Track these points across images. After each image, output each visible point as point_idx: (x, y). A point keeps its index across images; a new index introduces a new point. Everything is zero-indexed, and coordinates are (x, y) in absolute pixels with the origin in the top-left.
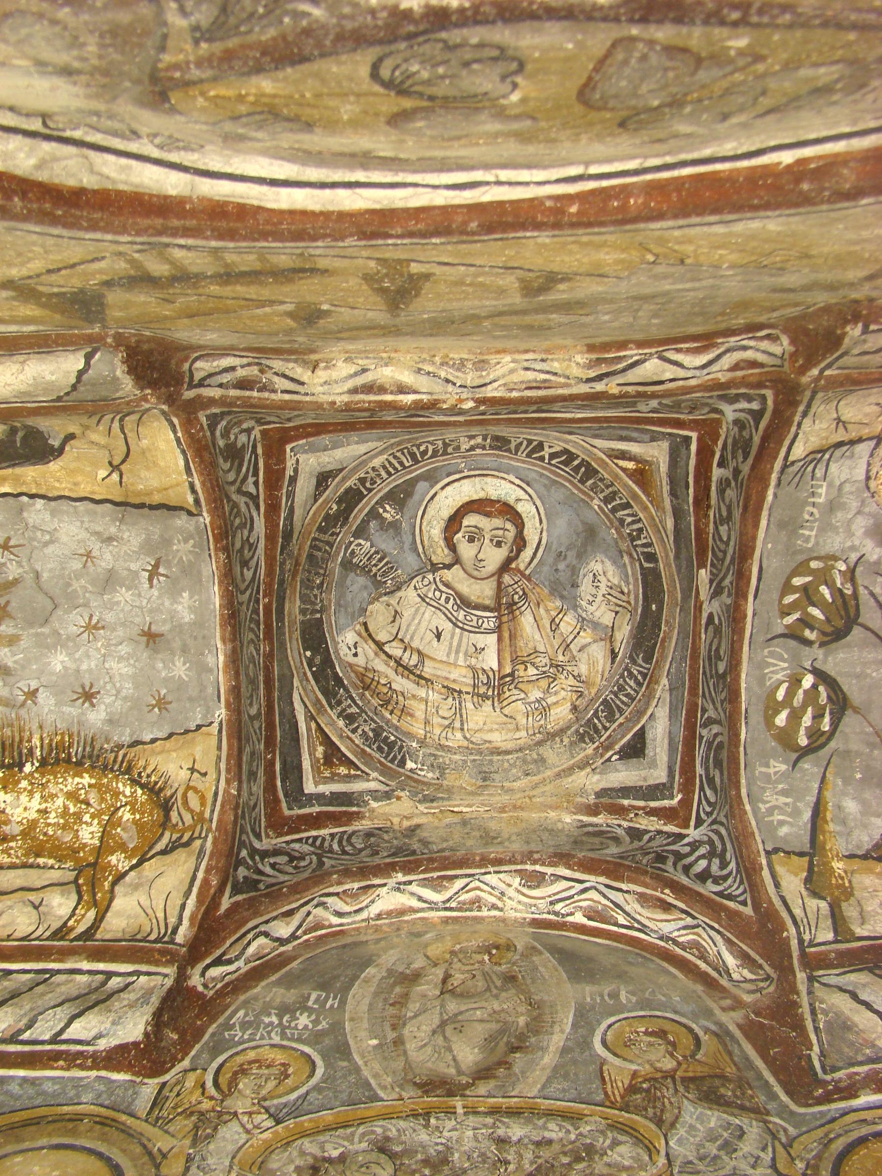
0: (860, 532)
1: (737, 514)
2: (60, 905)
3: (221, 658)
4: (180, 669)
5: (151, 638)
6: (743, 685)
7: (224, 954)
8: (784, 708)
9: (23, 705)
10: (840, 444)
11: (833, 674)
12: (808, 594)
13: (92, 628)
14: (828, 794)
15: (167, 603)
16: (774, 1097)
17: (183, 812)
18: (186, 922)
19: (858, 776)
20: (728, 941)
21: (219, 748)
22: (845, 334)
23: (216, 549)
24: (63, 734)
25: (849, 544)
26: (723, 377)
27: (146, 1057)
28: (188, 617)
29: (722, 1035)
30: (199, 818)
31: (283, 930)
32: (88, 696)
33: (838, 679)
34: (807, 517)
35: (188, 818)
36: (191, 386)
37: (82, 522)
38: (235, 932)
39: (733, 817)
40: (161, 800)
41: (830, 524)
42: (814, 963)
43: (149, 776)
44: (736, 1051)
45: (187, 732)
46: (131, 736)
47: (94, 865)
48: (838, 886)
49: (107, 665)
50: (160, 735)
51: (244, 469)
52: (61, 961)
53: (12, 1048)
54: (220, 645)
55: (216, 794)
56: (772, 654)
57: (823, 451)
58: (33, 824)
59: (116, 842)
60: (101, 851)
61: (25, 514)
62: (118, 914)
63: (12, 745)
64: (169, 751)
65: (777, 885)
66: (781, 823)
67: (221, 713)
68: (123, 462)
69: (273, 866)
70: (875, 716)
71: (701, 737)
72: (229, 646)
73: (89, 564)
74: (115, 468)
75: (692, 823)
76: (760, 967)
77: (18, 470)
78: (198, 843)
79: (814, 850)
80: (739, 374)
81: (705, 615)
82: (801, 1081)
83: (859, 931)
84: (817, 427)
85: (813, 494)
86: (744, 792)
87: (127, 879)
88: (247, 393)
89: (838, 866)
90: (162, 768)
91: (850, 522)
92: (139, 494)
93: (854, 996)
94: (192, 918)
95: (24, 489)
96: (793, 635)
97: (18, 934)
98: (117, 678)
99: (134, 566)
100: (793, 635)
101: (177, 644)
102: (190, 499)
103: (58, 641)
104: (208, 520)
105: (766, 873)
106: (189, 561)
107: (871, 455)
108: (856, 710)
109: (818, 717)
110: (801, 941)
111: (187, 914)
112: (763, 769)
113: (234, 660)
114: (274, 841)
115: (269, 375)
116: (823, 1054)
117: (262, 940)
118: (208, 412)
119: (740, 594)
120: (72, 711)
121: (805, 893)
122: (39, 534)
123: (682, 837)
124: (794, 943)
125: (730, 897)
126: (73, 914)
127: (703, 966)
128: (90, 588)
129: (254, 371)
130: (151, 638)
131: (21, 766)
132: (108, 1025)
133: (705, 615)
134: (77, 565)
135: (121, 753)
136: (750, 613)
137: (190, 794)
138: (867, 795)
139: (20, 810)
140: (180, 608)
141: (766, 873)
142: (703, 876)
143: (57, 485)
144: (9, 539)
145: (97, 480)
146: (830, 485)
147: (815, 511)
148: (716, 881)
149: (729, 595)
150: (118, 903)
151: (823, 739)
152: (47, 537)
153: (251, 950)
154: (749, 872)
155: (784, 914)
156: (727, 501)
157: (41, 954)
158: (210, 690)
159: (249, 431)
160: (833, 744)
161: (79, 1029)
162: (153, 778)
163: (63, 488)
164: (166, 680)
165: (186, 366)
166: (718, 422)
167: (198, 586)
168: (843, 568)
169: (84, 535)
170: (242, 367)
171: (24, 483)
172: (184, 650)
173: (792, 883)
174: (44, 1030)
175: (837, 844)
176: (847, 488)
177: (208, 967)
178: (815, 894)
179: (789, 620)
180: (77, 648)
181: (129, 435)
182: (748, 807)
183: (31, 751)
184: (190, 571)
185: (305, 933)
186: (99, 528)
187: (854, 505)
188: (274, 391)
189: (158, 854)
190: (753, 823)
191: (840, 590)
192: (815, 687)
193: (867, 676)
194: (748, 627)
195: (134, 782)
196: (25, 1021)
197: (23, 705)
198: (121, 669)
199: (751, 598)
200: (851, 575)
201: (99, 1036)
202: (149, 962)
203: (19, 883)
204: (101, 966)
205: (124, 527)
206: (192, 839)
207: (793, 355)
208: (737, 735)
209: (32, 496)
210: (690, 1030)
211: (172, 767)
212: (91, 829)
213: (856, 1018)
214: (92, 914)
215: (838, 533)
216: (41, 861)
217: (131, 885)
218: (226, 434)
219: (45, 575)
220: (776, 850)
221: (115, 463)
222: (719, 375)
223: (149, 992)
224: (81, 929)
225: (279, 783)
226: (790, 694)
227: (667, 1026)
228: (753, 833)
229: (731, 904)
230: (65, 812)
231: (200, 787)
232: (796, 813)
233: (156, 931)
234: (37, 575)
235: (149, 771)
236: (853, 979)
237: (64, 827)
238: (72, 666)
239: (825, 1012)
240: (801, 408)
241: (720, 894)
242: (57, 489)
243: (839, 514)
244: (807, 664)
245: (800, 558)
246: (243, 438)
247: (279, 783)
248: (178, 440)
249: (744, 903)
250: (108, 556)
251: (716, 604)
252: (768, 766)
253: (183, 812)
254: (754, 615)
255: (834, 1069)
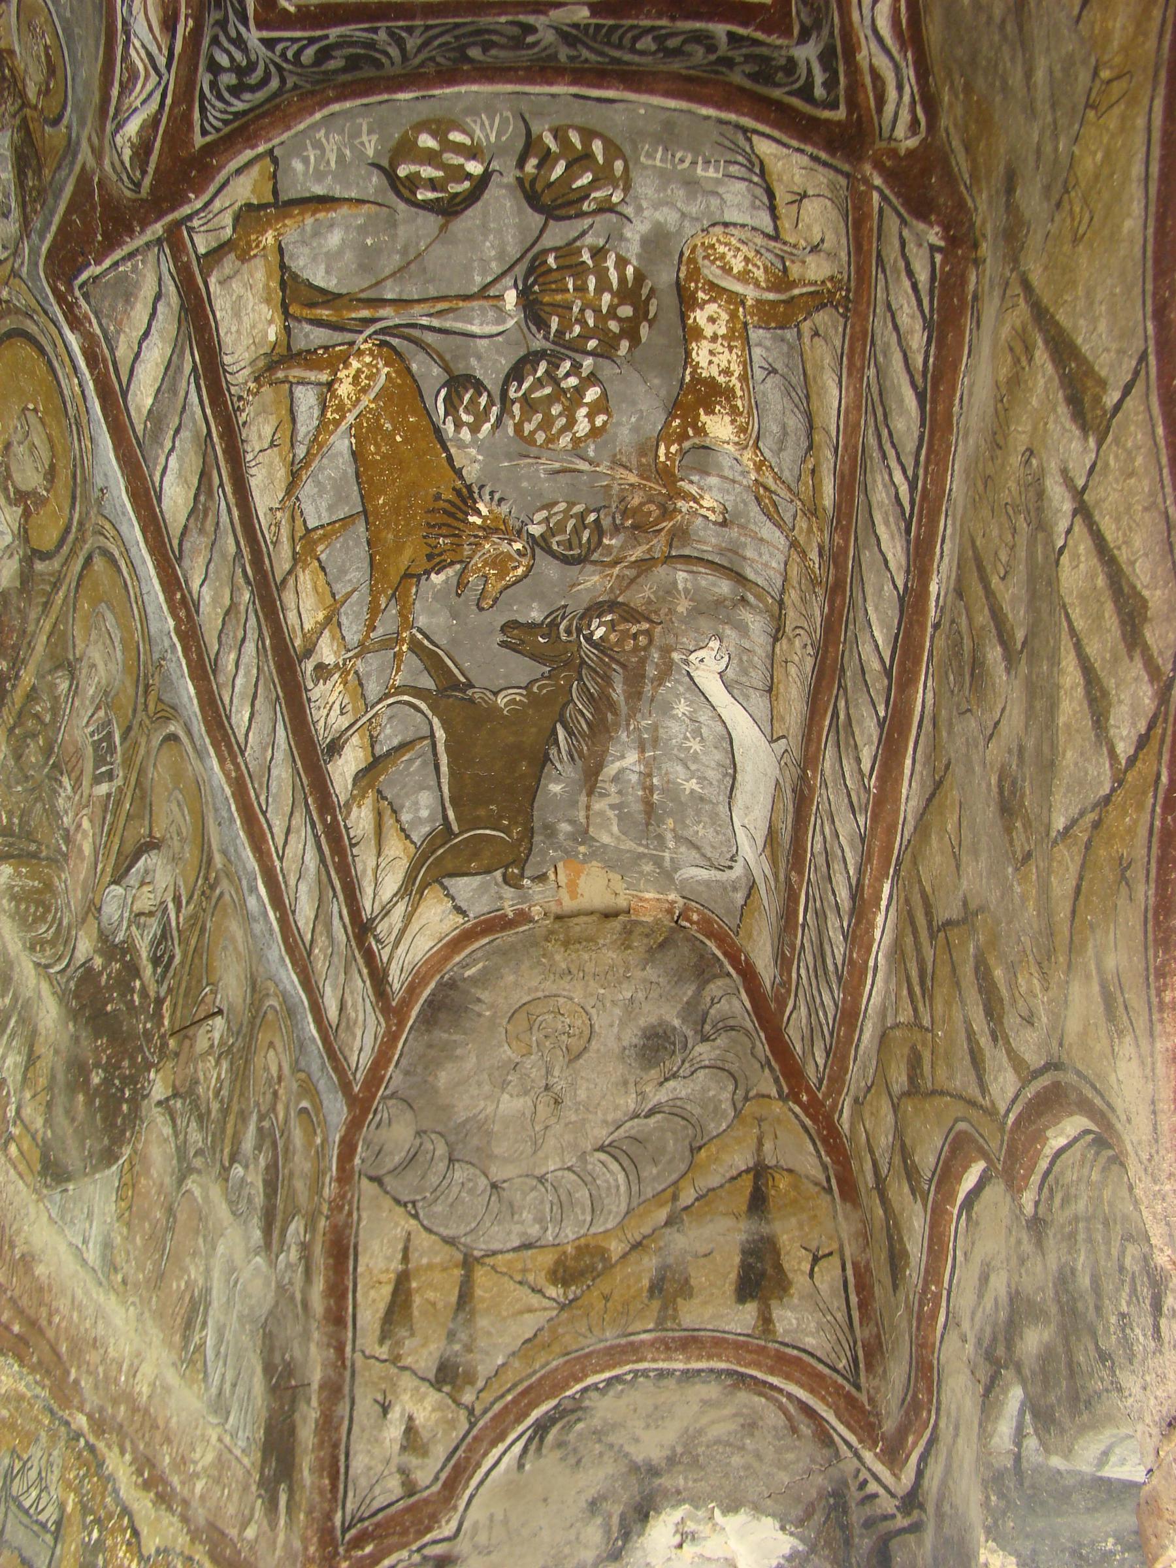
0: (659, 216)
1: (676, 66)
6: (463, 89)
8: (440, 143)
10: (771, 195)
11: (486, 196)
12: (583, 159)
14: (345, 210)
16: (42, 238)
19: (369, 242)
20: (155, 121)
22: (931, 225)
25: (645, 204)
26: (862, 57)
29: (71, 148)
33: (479, 204)
34: (679, 155)
39: (302, 98)
41: (669, 182)
42: (174, 240)
44: (64, 173)
48: (249, 243)
56: (504, 121)
57: (762, 174)
65: (239, 172)
66: (306, 161)
70: (438, 250)
71: (375, 30)
75: (266, 34)
76: (144, 172)
79: (282, 205)
80: (868, 80)
81: (531, 19)
82: (65, 262)
83: (212, 280)
84: (796, 171)
85: (707, 162)
86: (336, 107)
89: (269, 238)
91: (673, 205)
93: (158, 297)
96: (531, 144)
100: (531, 144)
105: (249, 154)
107: (754, 229)
108: (443, 228)
109: (433, 184)
110: (190, 217)
112: (365, 128)
116: (96, 279)
119: (579, 75)
121: (236, 207)
123: (244, 21)
124: (186, 210)
125: (203, 110)
127: (115, 92)
133: (531, 19)
136: (555, 89)
138: (348, 255)
141: (249, 154)
142: (214, 68)
146: (718, 182)
147: (686, 164)
148: (214, 85)
149: (571, 59)
151: (406, 193)
154: (242, 131)
155: (212, 189)
156: (688, 48)
160: (402, 206)
166: (788, 33)
168: (615, 199)
173: (244, 189)
175: (291, 231)
176: (715, 202)
178: (237, 219)
179: (549, 140)
182: (318, 116)
187: (693, 210)
190: (301, 127)
191: (587, 196)
192: (469, 176)
193: (486, 236)
194: (537, 89)
199: (574, 90)
200: (606, 208)
207: (894, 153)
208: (401, 88)
210: (64, 107)
213: (139, 306)
215: (658, 191)
220: (275, 161)
222: (864, 52)
226: (458, 148)
227: (59, 73)
228: (289, 128)
229: (197, 115)
232: (319, 176)
236: (170, 288)
239: (135, 269)
240: (823, 155)
241: (202, 96)
243: (681, 193)
244: (495, 165)
245: (627, 149)
249: (204, 133)
251: (550, 37)
252: (369, 133)
254: (553, 96)
255: (86, 296)
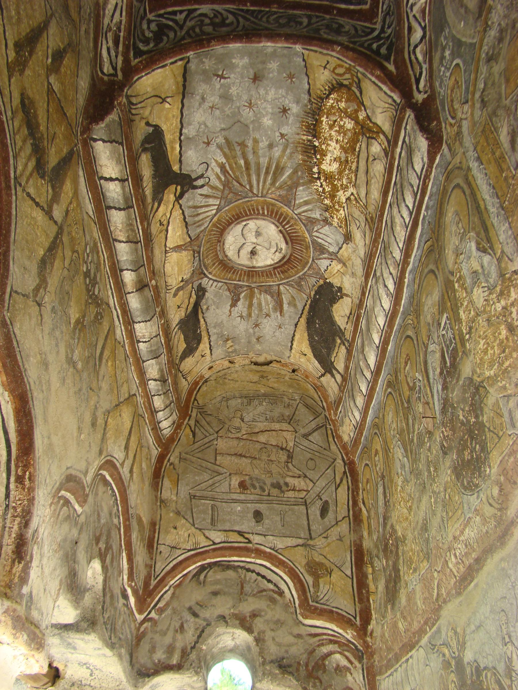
2: (376, 148)
3: (269, 44)
4: (273, 65)
5: (256, 78)
7: (415, 76)
9: (287, 140)
13: (250, 105)
15: (238, 70)
17: (344, 77)
18: (392, 94)
21: (316, 51)
23: (209, 47)
24: (302, 125)
27: (435, 142)
28: (246, 60)
30: (348, 70)
31: (418, 34)
32: (285, 111)
35: (348, 76)
36: (116, 75)
37: (194, 112)
38: (407, 67)
40: (337, 87)
43: (325, 90)
45: (306, 66)
46: (305, 94)
47: (362, 127)
49: (270, 100)
50: (306, 80)
51: (171, 23)
52: (395, 159)
53: (418, 197)
54: (262, 45)
55: (338, 58)
58: (342, 147)
59: (354, 113)
60: (357, 122)
61: (191, 136)
62: (383, 124)
63: (306, 148)
64: (315, 78)
67: (298, 48)
68: (160, 97)
69: (389, 27)
72: (263, 39)
73: (217, 107)
74: (164, 100)
77: (167, 142)
78: (359, 75)
87: (369, 114)
88: (121, 39)
90: (323, 82)
92: (178, 88)
94: (392, 91)
95: (177, 139)
97: (383, 171)
98: (277, 96)
99: (218, 86)
101: (260, 66)
102: (180, 63)
103: (257, 121)
104: (192, 53)
106: (215, 60)
111: (388, 92)
113: (272, 36)
114: (379, 20)
115: (112, 25)
117: (418, 50)
118: (132, 59)
120: (291, 119)
122: (201, 130)
126: (380, 144)
128: (230, 106)
129: (110, 35)
130: (256, 78)
131: (315, 146)
132: (419, 154)
134: (217, 112)
135: (313, 100)
137: (337, 71)
139: (335, 151)
140: (241, 64)
143: (174, 124)
144: (204, 142)
145: (171, 108)
150: (379, 123)
152: (203, 126)
153: (420, 58)
157: (391, 166)
158: (285, 51)
159: (149, 22)
161: (418, 167)
162: (327, 88)
163: (176, 122)
164: (279, 72)
165: (106, 78)
167: (229, 55)
169: (201, 111)
170: (107, 43)
171: (174, 139)
172: (264, 63)
174: (415, 182)
177: (418, 88)
180: (260, 113)
181: (145, 98)
183: (309, 141)
184: (220, 59)
185: (424, 21)
186: (197, 104)
188: (121, 21)
189: (361, 95)
195: (327, 97)
196: (410, 187)
197: (287, 140)
198: (272, 94)
201: (422, 159)
202: (402, 122)
203: (364, 162)
204: (400, 143)
205: (196, 93)
206: (357, 77)
209: (181, 134)
211: (323, 77)
212: (347, 123)
214: (382, 136)
216: (357, 150)
217: (372, 114)
218: (146, 41)
219: (223, 126)
221: (161, 101)
223: (412, 128)
224: (386, 144)
225: (352, 7)
230: (338, 132)
231: (333, 65)
233: (393, 111)
234: (223, 129)
235: (323, 89)
237: (345, 134)
238: (269, 116)
242: (176, 124)
246: (153, 26)
247: (352, 7)
248: (146, 75)
250: (212, 99)
253: (344, 77)
